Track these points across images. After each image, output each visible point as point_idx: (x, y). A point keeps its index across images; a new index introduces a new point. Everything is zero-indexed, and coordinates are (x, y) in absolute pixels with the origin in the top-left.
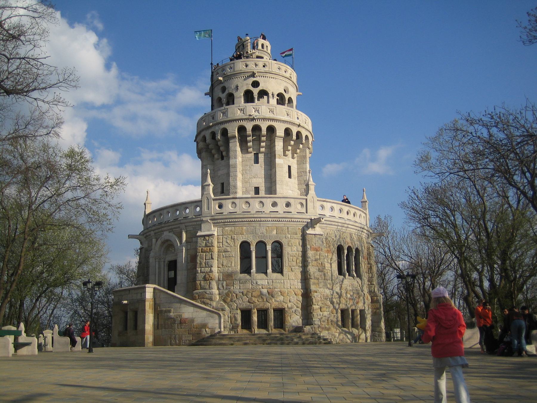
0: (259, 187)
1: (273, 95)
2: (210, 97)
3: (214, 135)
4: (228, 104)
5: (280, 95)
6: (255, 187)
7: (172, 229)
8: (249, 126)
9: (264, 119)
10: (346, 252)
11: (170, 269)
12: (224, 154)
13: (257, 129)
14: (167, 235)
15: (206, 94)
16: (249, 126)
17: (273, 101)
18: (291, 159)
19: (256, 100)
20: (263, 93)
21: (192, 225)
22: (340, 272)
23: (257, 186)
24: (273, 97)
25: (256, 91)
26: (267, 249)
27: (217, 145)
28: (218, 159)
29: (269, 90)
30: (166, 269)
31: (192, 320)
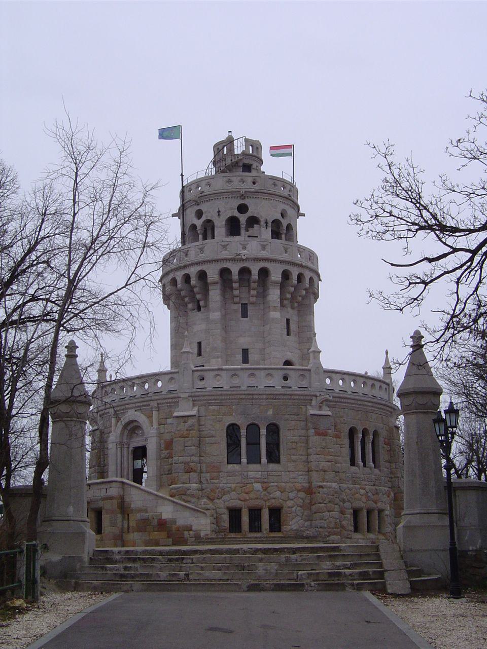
0: (248, 349)
1: (266, 223)
2: (179, 218)
3: (187, 278)
4: (205, 238)
5: (276, 223)
6: (243, 349)
7: (137, 407)
8: (235, 269)
9: (256, 259)
10: (360, 435)
11: (135, 458)
12: (202, 303)
13: (245, 271)
14: (131, 414)
15: (174, 215)
16: (235, 269)
17: (267, 233)
18: (289, 309)
19: (243, 231)
20: (253, 221)
21: (167, 403)
22: (353, 462)
23: (245, 347)
24: (267, 226)
25: (243, 218)
26: (261, 434)
27: (192, 291)
28: (193, 310)
29: (261, 216)
30: (131, 457)
31: (174, 521)
